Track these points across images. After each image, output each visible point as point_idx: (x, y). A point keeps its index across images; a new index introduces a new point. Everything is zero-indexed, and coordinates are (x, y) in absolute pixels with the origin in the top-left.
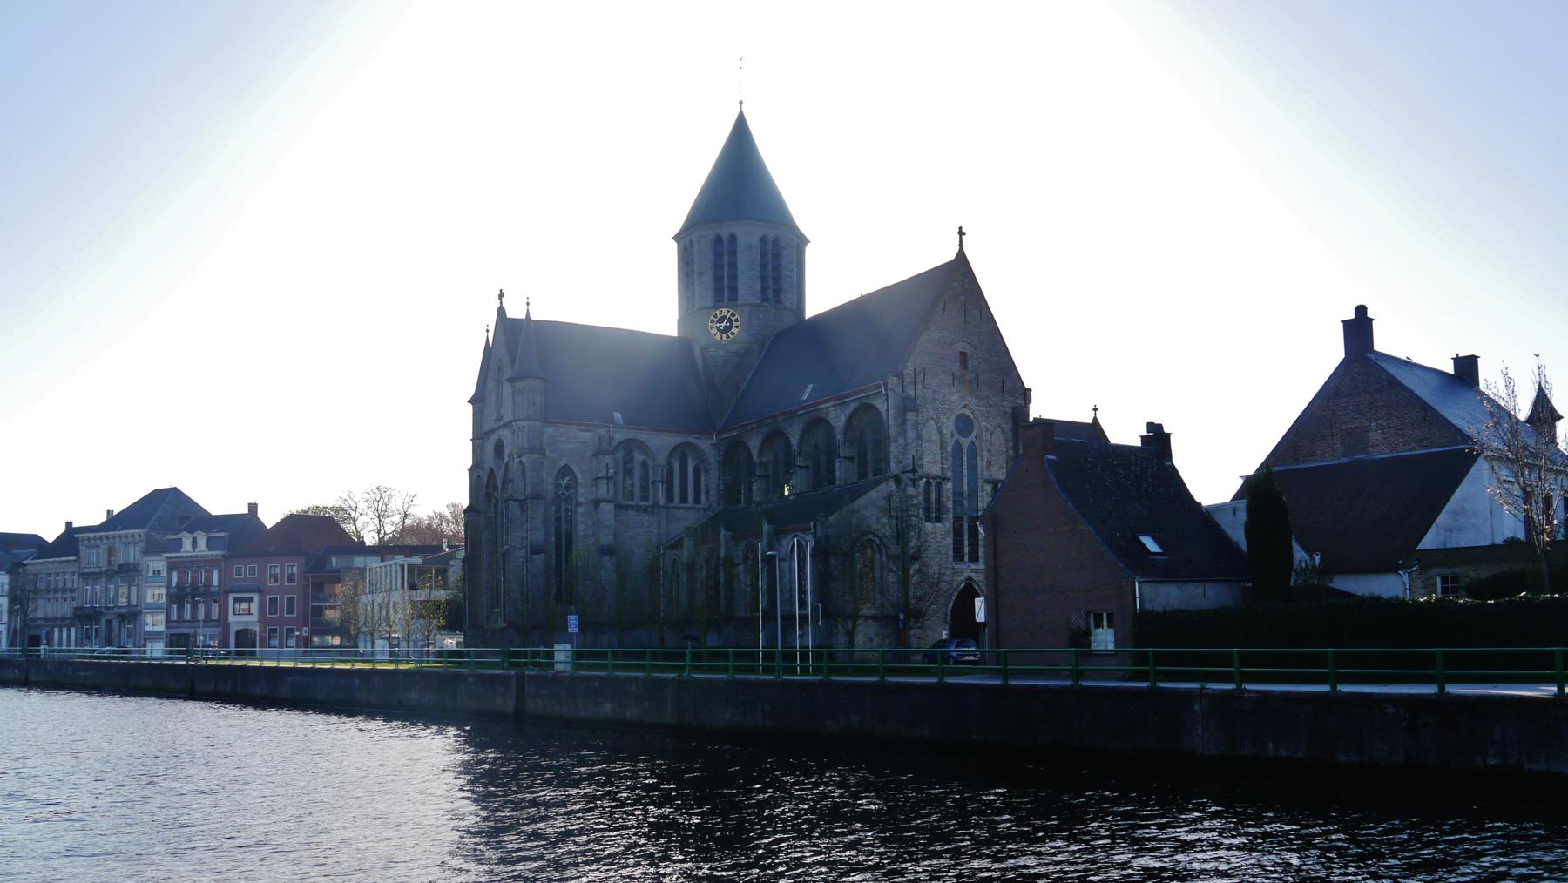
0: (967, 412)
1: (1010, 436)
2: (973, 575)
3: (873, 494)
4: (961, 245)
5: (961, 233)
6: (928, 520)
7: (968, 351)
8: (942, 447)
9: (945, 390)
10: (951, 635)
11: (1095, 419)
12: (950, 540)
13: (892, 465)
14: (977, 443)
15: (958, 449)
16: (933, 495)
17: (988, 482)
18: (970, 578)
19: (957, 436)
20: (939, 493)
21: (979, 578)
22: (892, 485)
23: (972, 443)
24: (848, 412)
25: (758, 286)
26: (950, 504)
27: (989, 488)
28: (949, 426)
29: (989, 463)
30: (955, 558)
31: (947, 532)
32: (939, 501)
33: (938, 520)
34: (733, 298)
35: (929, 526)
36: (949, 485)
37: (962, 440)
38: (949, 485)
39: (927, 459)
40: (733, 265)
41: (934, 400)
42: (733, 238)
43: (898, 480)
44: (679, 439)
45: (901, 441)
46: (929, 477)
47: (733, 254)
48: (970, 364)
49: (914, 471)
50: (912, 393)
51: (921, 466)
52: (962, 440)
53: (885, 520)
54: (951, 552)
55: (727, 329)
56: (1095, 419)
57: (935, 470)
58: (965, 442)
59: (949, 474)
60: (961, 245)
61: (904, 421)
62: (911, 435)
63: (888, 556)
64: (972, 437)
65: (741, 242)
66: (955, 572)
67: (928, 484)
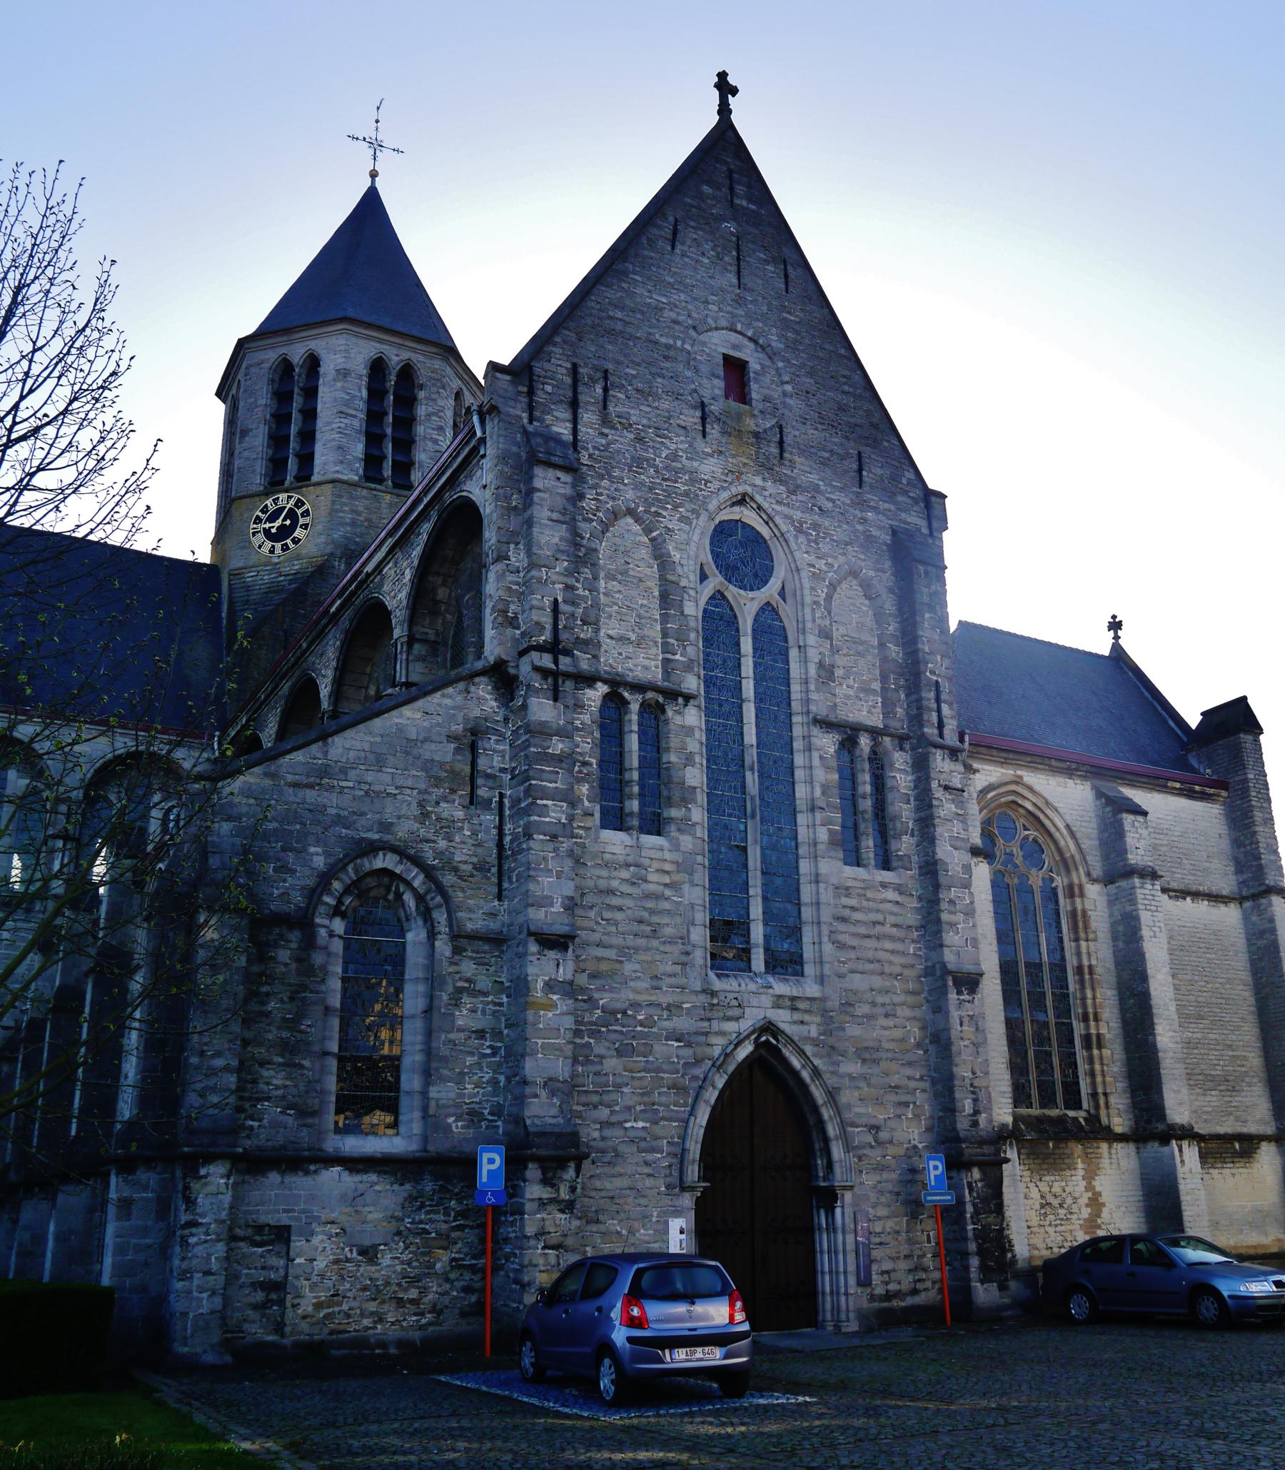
0: (749, 517)
1: (889, 605)
2: (782, 1018)
3: (410, 717)
4: (724, 110)
5: (725, 88)
6: (615, 819)
7: (746, 352)
8: (668, 597)
9: (677, 443)
10: (704, 1231)
11: (1117, 648)
12: (696, 894)
13: (489, 633)
14: (786, 611)
15: (719, 619)
16: (633, 742)
17: (827, 725)
18: (769, 1028)
19: (716, 580)
20: (654, 739)
21: (298, 529)
22: (484, 698)
23: (768, 608)
24: (417, 552)
25: (359, 449)
26: (695, 776)
27: (828, 743)
28: (691, 547)
29: (827, 672)
30: (717, 962)
31: (684, 867)
32: (654, 765)
33: (654, 825)
34: (304, 476)
35: (616, 842)
36: (692, 717)
37: (732, 592)
38: (692, 717)
39: (610, 628)
40: (310, 414)
41: (638, 463)
42: (313, 362)
43: (504, 680)
44: (123, 743)
45: (517, 557)
46: (616, 684)
47: (311, 393)
48: (755, 392)
49: (554, 648)
50: (564, 430)
51: (591, 645)
52: (732, 592)
53: (454, 810)
54: (700, 935)
55: (284, 532)
56: (1117, 648)
57: (644, 665)
58: (747, 604)
59: (692, 683)
60: (724, 110)
61: (528, 493)
62: (549, 537)
63: (460, 938)
64: (774, 585)
65: (328, 367)
66: (713, 1005)
67: (614, 702)
